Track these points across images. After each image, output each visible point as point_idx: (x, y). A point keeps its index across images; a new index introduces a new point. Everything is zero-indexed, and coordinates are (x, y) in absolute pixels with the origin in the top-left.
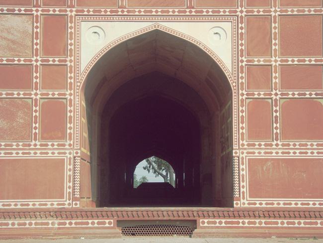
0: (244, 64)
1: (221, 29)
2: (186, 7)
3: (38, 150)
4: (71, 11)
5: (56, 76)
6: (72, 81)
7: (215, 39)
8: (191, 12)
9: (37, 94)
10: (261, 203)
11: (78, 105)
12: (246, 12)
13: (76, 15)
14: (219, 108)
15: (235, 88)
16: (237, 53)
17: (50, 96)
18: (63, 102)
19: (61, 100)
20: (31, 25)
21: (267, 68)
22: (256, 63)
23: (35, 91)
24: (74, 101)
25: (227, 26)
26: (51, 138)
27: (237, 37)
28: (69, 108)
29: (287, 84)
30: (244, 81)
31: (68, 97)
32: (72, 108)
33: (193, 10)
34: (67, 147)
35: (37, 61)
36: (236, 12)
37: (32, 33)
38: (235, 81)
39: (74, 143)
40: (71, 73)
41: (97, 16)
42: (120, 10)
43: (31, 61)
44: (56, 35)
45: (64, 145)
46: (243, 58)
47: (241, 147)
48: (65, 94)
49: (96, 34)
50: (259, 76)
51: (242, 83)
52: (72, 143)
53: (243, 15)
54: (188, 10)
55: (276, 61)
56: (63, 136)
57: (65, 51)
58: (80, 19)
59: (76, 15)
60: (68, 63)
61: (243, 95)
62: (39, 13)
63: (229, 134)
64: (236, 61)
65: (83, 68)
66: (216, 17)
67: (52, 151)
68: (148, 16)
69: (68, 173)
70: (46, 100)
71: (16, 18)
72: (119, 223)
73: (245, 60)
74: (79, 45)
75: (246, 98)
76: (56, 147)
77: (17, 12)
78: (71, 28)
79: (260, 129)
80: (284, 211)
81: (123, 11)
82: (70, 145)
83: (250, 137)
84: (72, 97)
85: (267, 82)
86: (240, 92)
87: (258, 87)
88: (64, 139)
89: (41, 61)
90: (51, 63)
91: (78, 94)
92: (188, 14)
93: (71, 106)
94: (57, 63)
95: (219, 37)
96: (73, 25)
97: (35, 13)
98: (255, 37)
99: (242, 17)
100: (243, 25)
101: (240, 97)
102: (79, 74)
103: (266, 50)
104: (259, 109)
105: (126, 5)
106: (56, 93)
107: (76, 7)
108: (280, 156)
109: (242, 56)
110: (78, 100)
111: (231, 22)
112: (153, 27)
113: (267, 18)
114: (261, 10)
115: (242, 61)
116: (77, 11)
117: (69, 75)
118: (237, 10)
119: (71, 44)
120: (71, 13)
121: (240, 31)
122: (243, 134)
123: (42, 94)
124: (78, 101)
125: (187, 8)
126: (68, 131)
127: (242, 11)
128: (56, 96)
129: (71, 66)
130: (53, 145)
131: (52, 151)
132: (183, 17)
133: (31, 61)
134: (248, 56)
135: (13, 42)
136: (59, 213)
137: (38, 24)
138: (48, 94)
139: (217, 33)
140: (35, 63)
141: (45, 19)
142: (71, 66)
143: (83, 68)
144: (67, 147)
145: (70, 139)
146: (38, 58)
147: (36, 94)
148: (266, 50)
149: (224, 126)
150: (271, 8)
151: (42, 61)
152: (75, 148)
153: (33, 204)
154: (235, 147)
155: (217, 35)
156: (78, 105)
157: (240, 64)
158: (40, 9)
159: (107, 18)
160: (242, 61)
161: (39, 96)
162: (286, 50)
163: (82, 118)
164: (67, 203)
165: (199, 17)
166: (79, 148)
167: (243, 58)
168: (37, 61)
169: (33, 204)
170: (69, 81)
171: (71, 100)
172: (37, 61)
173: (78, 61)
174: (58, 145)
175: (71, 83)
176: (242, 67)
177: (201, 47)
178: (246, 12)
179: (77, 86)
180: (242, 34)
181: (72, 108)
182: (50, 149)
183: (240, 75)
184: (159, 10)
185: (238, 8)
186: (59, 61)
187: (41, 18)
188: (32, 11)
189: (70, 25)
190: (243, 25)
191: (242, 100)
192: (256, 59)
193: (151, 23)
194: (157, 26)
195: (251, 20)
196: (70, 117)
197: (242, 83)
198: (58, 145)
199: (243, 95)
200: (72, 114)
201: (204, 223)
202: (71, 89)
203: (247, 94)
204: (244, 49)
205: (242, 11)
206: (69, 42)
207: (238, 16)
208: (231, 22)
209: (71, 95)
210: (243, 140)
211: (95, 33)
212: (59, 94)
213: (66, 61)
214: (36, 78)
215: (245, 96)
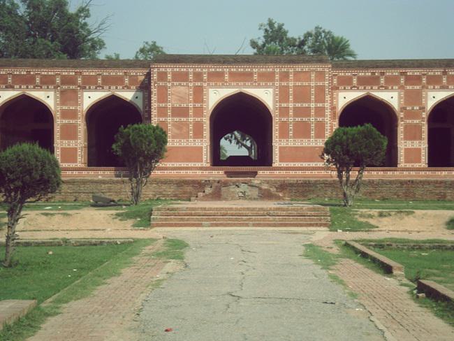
3: (192, 143)
5: (199, 112)
7: (266, 95)
9: (191, 119)
10: (284, 165)
16: (275, 102)
21: (287, 108)
27: (275, 95)
29: (295, 115)
35: (191, 105)
41: (216, 86)
44: (199, 94)
50: (284, 112)
55: (291, 105)
57: (202, 101)
66: (267, 86)
67: (198, 143)
69: (204, 152)
72: (226, 173)
79: (284, 134)
80: (293, 167)
83: (280, 138)
85: (287, 115)
87: (284, 116)
98: (283, 95)
103: (287, 101)
104: (284, 126)
108: (292, 145)
113: (288, 87)
120: (205, 85)
127: (277, 84)
131: (198, 143)
135: (182, 97)
136: (201, 168)
148: (287, 101)
153: (191, 164)
154: (273, 141)
159: (220, 87)
162: (295, 101)
164: (204, 164)
165: (259, 86)
169: (191, 164)
173: (208, 105)
201: (260, 173)
205: (277, 84)
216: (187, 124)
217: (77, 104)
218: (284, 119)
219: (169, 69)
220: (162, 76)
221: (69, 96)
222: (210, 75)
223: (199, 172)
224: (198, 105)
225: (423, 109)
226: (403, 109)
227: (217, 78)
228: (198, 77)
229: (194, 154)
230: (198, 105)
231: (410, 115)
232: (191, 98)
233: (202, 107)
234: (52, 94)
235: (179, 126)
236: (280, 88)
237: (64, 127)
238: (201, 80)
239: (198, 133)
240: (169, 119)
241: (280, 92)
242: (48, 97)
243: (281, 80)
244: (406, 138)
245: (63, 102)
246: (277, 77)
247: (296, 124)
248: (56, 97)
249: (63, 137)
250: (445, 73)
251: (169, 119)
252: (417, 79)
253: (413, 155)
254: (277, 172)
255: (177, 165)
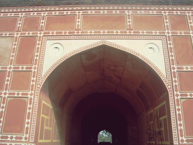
0: (175, 70)
1: (155, 45)
2: (126, 29)
4: (40, 33)
5: (21, 80)
6: (34, 83)
8: (130, 32)
9: (6, 93)
11: (36, 103)
12: (171, 33)
13: (44, 36)
14: (145, 110)
15: (170, 90)
16: (169, 63)
17: (16, 95)
18: (25, 101)
19: (23, 99)
20: (12, 43)
22: (185, 70)
23: (5, 91)
24: (34, 100)
25: (159, 43)
26: (12, 131)
28: (29, 106)
30: (177, 84)
31: (29, 96)
32: (31, 106)
33: (132, 31)
34: (23, 140)
35: (10, 68)
36: (165, 33)
37: (11, 49)
38: (170, 84)
39: (29, 136)
40: (34, 77)
41: (60, 36)
42: (76, 32)
43: (6, 68)
44: (27, 50)
45: (21, 138)
46: (174, 66)
47: (181, 143)
48: (27, 94)
49: (57, 49)
51: (176, 86)
52: (28, 136)
53: (170, 35)
54: (128, 31)
56: (21, 131)
57: (31, 61)
58: (46, 39)
59: (44, 36)
60: (33, 70)
61: (177, 95)
62: (18, 36)
63: (163, 129)
64: (169, 68)
65: (44, 73)
66: (149, 36)
68: (97, 35)
70: (12, 98)
71: (3, 39)
73: (176, 67)
74: (43, 56)
75: (181, 98)
76: (14, 139)
77: (4, 35)
78: (39, 44)
81: (78, 32)
82: (26, 138)
84: (32, 97)
86: (175, 93)
88: (21, 133)
89: (14, 68)
90: (20, 69)
91: (37, 94)
92: (128, 33)
93: (30, 104)
94: (24, 69)
95: (153, 51)
96: (40, 42)
97: (15, 36)
99: (169, 37)
100: (171, 42)
101: (176, 98)
102: (40, 78)
105: (80, 28)
106: (21, 93)
107: (44, 30)
109: (173, 64)
110: (37, 99)
111: (162, 40)
112: (101, 43)
114: (183, 32)
115: (174, 68)
116: (44, 33)
117: (32, 79)
118: (165, 32)
119: (37, 56)
120: (40, 34)
121: (169, 46)
122: (181, 130)
123: (9, 94)
124: (37, 100)
125: (127, 30)
126: (26, 125)
128: (20, 95)
129: (34, 72)
130: (12, 138)
132: (124, 36)
133: (6, 68)
134: (177, 64)
137: (16, 43)
138: (14, 94)
139: (151, 48)
140: (8, 70)
141: (22, 39)
142: (34, 72)
143: (44, 73)
144: (23, 140)
145: (27, 133)
146: (12, 66)
147: (5, 94)
149: (152, 122)
150: (190, 31)
151: (14, 68)
152: (30, 141)
155: (152, 49)
156: (36, 103)
157: (173, 71)
158: (19, 33)
160: (174, 68)
161: (7, 95)
163: (42, 115)
165: (136, 36)
166: (33, 141)
167: (174, 66)
168: (10, 68)
170: (32, 83)
171: (31, 99)
172: (10, 68)
173: (40, 69)
174: (16, 138)
175: (33, 85)
176: (174, 72)
177: (141, 58)
178: (171, 33)
179: (38, 88)
180: (171, 48)
181: (31, 106)
182: (9, 141)
183: (174, 79)
184: (106, 31)
185: (165, 30)
186: (26, 68)
187: (19, 39)
188: (14, 34)
189: (38, 42)
190: (171, 42)
191: (178, 100)
192: (184, 67)
193: (100, 40)
194: (104, 42)
196: (29, 113)
197: (176, 86)
198: (16, 138)
199: (177, 95)
200: (31, 111)
202: (32, 90)
203: (181, 95)
204: (174, 59)
205: (169, 33)
206: (36, 54)
207: (166, 36)
208: (162, 40)
209: (31, 94)
210: (182, 136)
211: (57, 48)
212: (22, 94)
213: (31, 68)
214: (8, 81)
215: (179, 97)
222: (51, 20)
230: (23, 67)
232: (13, 56)
236: (174, 40)
241: (175, 47)
243: (174, 27)
246: (167, 22)
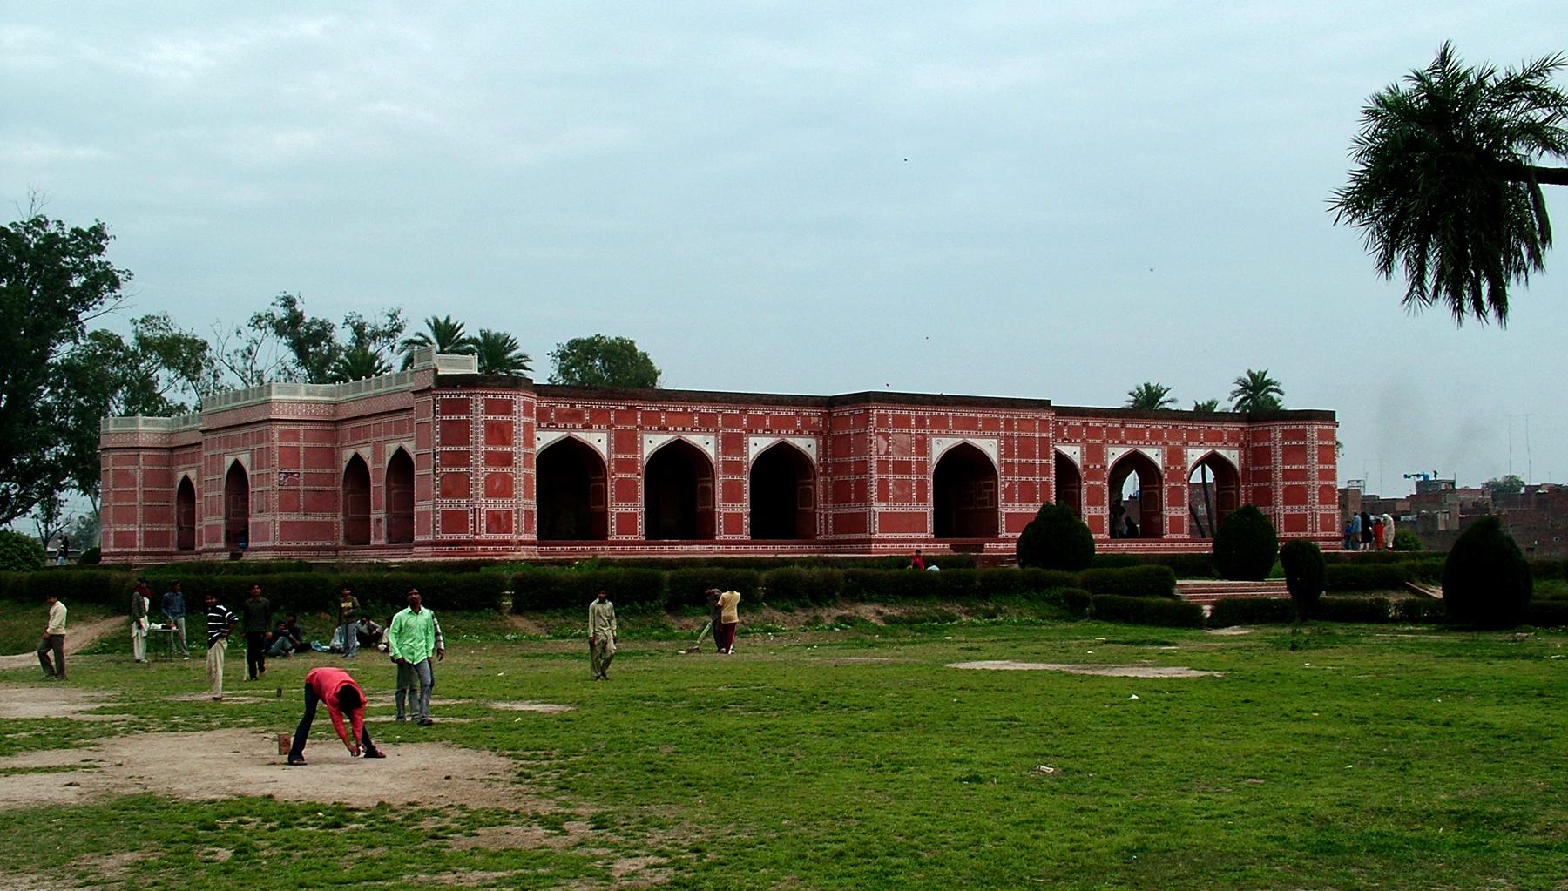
3: (916, 507)
5: (922, 467)
7: (990, 447)
27: (1000, 447)
41: (940, 435)
44: (922, 446)
50: (1009, 469)
68: (962, 435)
79: (1009, 498)
98: (1007, 450)
103: (1012, 456)
153: (914, 536)
169: (914, 536)
195: (1006, 438)
216: (909, 482)
217: (741, 453)
218: (883, 476)
219: (890, 412)
220: (882, 420)
221: (732, 444)
223: (923, 546)
224: (921, 459)
225: (1104, 467)
226: (1085, 467)
227: (939, 424)
228: (921, 422)
229: (915, 522)
230: (921, 459)
231: (1094, 475)
233: (925, 462)
234: (712, 439)
235: (902, 485)
237: (727, 484)
238: (924, 427)
239: (922, 498)
240: (891, 477)
242: (598, 440)
244: (726, 499)
245: (725, 452)
247: (1031, 485)
248: (717, 444)
249: (726, 499)
250: (1123, 425)
251: (891, 477)
252: (1095, 432)
253: (733, 523)
254: (1002, 546)
255: (899, 536)
